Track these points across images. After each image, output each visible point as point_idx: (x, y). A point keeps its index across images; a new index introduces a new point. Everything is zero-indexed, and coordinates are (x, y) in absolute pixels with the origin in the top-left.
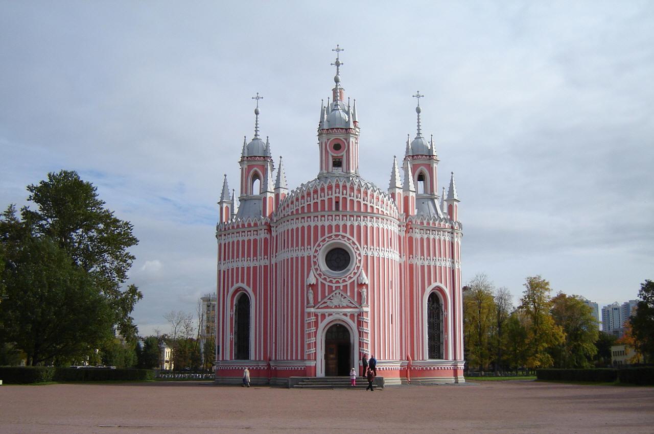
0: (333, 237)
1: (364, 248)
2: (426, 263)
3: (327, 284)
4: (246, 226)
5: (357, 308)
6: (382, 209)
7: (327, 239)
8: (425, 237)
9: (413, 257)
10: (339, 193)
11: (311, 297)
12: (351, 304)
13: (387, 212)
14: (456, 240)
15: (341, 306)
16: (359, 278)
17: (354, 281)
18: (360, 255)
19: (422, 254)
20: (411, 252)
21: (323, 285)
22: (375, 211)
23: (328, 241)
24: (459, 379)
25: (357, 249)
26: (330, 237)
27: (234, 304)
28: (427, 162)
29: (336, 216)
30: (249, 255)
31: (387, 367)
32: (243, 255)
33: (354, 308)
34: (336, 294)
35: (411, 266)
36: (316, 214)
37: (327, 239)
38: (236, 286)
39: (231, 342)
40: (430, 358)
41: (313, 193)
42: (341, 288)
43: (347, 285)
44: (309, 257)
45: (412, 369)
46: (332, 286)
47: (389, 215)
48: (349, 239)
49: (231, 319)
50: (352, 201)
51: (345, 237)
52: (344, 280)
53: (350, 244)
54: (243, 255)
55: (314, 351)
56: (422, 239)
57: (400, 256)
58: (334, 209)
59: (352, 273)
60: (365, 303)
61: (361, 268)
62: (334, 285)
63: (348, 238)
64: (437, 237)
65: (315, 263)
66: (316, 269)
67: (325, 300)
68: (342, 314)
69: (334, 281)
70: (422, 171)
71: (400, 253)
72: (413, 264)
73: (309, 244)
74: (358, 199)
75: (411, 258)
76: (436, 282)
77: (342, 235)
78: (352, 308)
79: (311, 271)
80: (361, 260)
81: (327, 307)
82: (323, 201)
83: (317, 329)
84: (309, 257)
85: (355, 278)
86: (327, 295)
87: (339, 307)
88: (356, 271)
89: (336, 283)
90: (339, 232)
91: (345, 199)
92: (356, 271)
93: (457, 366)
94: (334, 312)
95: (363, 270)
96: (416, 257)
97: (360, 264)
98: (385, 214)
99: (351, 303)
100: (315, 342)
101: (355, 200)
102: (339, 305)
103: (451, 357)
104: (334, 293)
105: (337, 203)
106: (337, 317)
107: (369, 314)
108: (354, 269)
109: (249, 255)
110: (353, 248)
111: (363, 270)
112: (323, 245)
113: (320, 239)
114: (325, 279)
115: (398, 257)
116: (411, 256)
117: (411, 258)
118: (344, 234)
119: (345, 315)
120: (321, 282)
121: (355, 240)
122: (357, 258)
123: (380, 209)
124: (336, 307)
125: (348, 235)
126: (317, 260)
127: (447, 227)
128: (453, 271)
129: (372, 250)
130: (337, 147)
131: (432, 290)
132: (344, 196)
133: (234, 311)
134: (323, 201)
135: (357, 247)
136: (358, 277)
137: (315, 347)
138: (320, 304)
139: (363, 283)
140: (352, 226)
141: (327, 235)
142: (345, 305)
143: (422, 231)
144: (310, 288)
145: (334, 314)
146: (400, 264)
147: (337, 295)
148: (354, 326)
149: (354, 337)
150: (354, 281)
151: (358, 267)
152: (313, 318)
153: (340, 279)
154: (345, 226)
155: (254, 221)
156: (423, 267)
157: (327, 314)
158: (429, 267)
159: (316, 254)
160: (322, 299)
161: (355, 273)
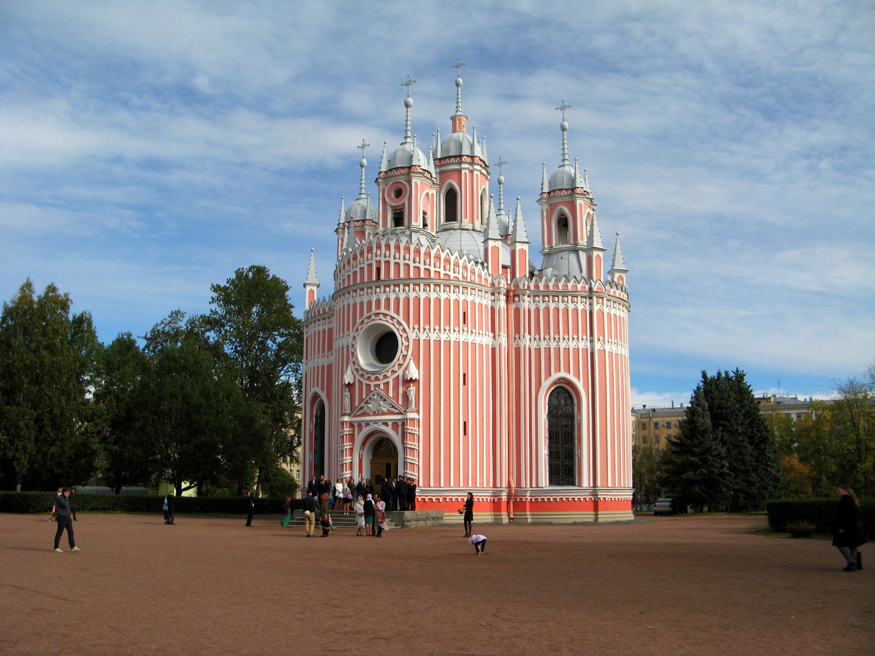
0: (373, 317)
1: (414, 328)
2: (543, 345)
3: (365, 382)
4: (321, 313)
5: (400, 413)
6: (447, 272)
7: (366, 321)
8: (542, 306)
9: (519, 338)
10: (380, 256)
11: (347, 401)
12: (393, 409)
13: (456, 275)
14: (596, 308)
15: (380, 413)
17: (399, 375)
18: (407, 339)
19: (538, 331)
20: (517, 331)
21: (360, 383)
22: (432, 276)
23: (367, 323)
24: (599, 516)
25: (404, 330)
26: (369, 317)
27: (314, 415)
28: (567, 199)
29: (376, 287)
30: (323, 352)
31: (485, 498)
32: (319, 353)
35: (518, 350)
36: (354, 288)
37: (366, 321)
38: (313, 390)
39: (310, 464)
40: (552, 482)
41: (353, 259)
42: (382, 387)
43: (388, 382)
44: (348, 346)
45: (518, 500)
46: (370, 385)
47: (461, 278)
48: (392, 318)
49: (311, 433)
50: (397, 265)
51: (388, 315)
52: (386, 375)
53: (393, 324)
54: (319, 353)
56: (537, 310)
57: (494, 337)
58: (374, 278)
59: (396, 366)
60: (413, 406)
61: (409, 356)
62: (372, 384)
63: (391, 316)
64: (562, 306)
65: (353, 353)
66: (354, 363)
67: (362, 405)
68: (380, 423)
69: (373, 378)
70: (562, 212)
71: (493, 331)
72: (520, 347)
73: (348, 329)
74: (407, 262)
75: (518, 339)
76: (560, 371)
77: (383, 314)
79: (349, 366)
80: (408, 345)
81: (365, 414)
82: (362, 269)
83: (353, 445)
84: (348, 346)
85: (400, 373)
86: (364, 396)
87: (379, 414)
88: (401, 362)
89: (374, 381)
90: (380, 309)
91: (387, 263)
92: (401, 362)
93: (597, 495)
94: (371, 421)
95: (412, 361)
96: (524, 336)
98: (452, 278)
99: (393, 407)
100: (351, 463)
101: (402, 262)
102: (378, 411)
103: (586, 482)
104: (371, 395)
105: (378, 270)
106: (375, 426)
109: (323, 352)
110: (398, 330)
111: (412, 361)
112: (361, 329)
113: (358, 321)
114: (362, 376)
115: (492, 339)
116: (517, 336)
117: (518, 339)
118: (386, 312)
119: (386, 424)
120: (358, 380)
121: (401, 319)
122: (403, 344)
123: (442, 272)
124: (374, 414)
125: (392, 313)
126: (355, 350)
127: (579, 289)
128: (592, 354)
129: (427, 331)
130: (399, 193)
131: (555, 383)
132: (387, 259)
133: (314, 423)
134: (362, 269)
135: (404, 328)
137: (351, 469)
138: (357, 409)
139: (409, 379)
140: (397, 300)
141: (366, 315)
142: (385, 410)
143: (537, 299)
144: (347, 389)
145: (371, 423)
146: (493, 350)
147: (375, 397)
148: (397, 439)
150: (399, 375)
151: (405, 357)
152: (348, 429)
153: (381, 373)
154: (388, 300)
155: (328, 305)
156: (538, 350)
157: (363, 424)
158: (548, 350)
159: (354, 342)
160: (360, 402)
161: (400, 365)
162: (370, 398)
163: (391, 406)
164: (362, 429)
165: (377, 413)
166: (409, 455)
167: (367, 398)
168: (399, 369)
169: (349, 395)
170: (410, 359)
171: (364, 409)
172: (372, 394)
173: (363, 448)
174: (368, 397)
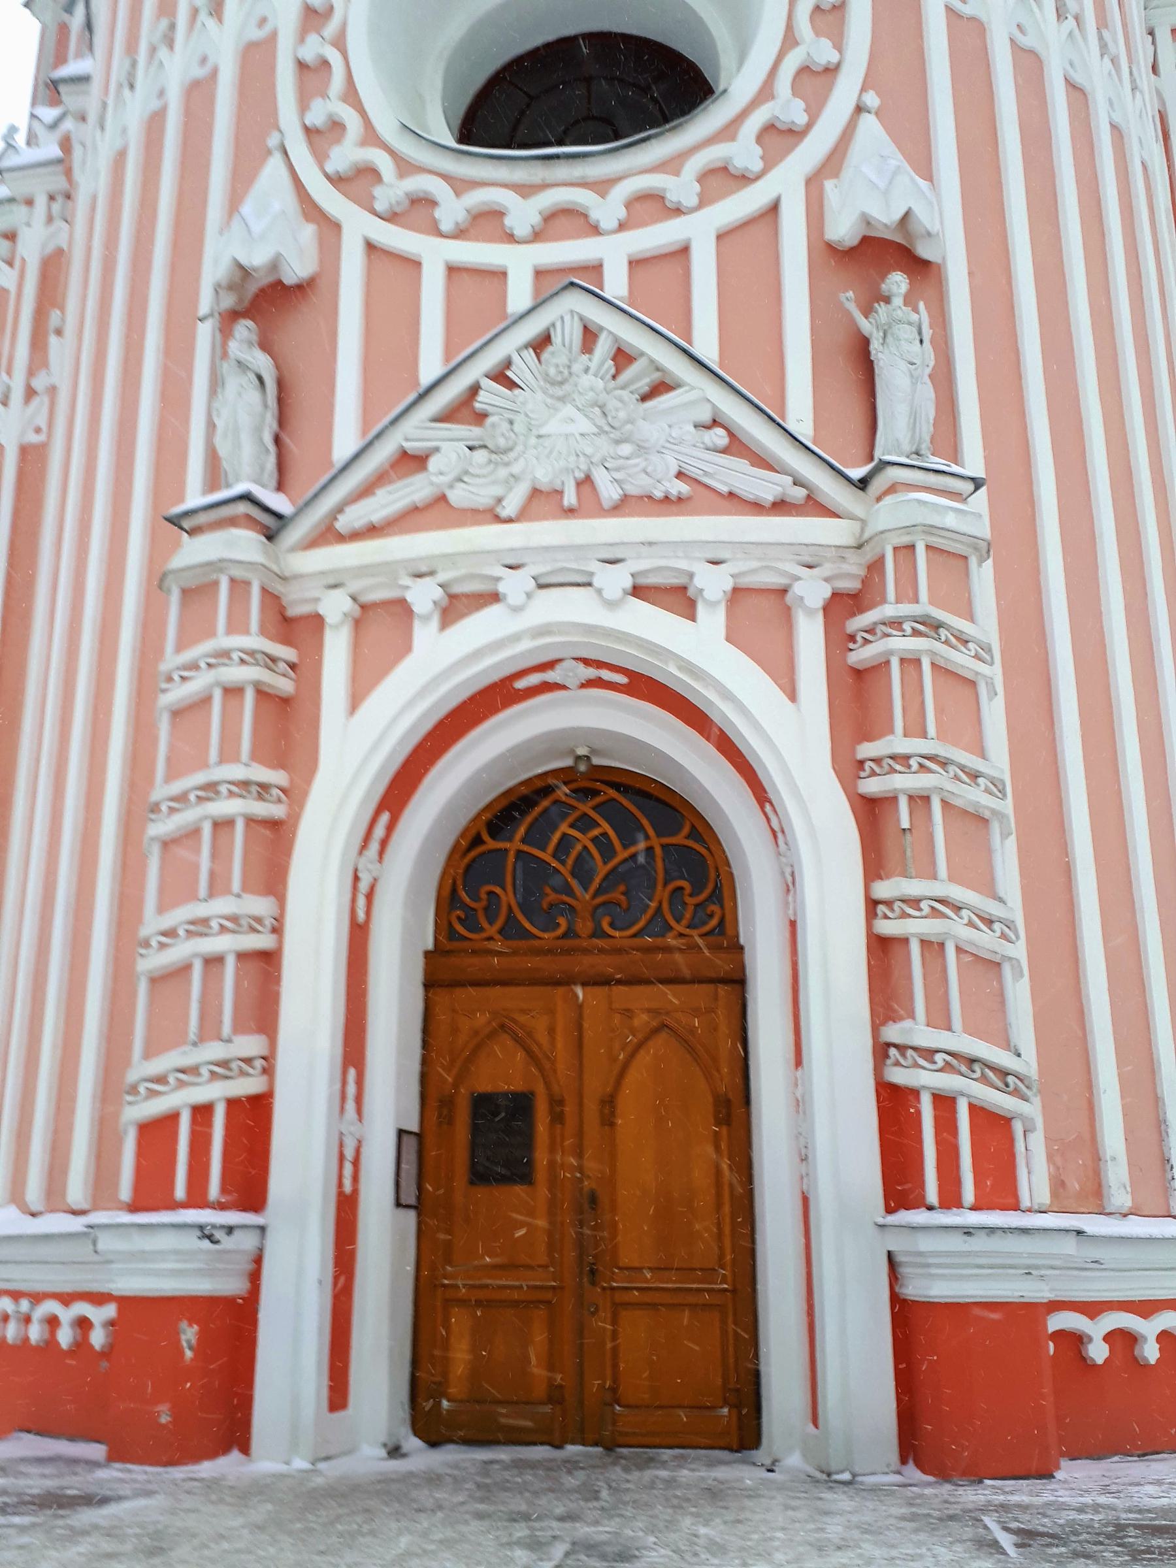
5: (814, 506)
15: (609, 492)
16: (829, 185)
17: (774, 209)
33: (781, 506)
34: (541, 343)
42: (616, 284)
43: (684, 251)
55: (248, 1086)
78: (756, 507)
79: (273, 171)
83: (295, 795)
86: (430, 367)
95: (868, 122)
97: (839, 47)
99: (737, 446)
102: (586, 483)
107: (983, 577)
108: (766, 92)
111: (869, 124)
120: (371, 247)
136: (814, 183)
149: (790, 885)
150: (774, 209)
152: (254, 641)
162: (501, 376)
163: (719, 437)
164: (407, 648)
165: (570, 498)
166: (952, 879)
167: (475, 372)
168: (770, 163)
169: (262, 362)
170: (859, 109)
171: (433, 464)
172: (530, 330)
173: (390, 828)
174: (489, 360)
